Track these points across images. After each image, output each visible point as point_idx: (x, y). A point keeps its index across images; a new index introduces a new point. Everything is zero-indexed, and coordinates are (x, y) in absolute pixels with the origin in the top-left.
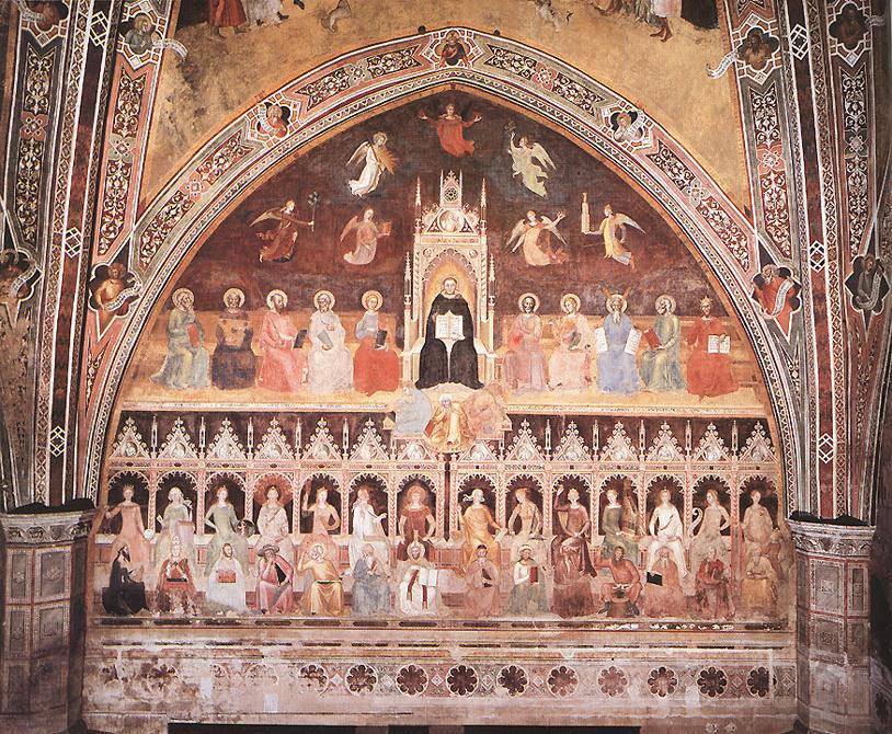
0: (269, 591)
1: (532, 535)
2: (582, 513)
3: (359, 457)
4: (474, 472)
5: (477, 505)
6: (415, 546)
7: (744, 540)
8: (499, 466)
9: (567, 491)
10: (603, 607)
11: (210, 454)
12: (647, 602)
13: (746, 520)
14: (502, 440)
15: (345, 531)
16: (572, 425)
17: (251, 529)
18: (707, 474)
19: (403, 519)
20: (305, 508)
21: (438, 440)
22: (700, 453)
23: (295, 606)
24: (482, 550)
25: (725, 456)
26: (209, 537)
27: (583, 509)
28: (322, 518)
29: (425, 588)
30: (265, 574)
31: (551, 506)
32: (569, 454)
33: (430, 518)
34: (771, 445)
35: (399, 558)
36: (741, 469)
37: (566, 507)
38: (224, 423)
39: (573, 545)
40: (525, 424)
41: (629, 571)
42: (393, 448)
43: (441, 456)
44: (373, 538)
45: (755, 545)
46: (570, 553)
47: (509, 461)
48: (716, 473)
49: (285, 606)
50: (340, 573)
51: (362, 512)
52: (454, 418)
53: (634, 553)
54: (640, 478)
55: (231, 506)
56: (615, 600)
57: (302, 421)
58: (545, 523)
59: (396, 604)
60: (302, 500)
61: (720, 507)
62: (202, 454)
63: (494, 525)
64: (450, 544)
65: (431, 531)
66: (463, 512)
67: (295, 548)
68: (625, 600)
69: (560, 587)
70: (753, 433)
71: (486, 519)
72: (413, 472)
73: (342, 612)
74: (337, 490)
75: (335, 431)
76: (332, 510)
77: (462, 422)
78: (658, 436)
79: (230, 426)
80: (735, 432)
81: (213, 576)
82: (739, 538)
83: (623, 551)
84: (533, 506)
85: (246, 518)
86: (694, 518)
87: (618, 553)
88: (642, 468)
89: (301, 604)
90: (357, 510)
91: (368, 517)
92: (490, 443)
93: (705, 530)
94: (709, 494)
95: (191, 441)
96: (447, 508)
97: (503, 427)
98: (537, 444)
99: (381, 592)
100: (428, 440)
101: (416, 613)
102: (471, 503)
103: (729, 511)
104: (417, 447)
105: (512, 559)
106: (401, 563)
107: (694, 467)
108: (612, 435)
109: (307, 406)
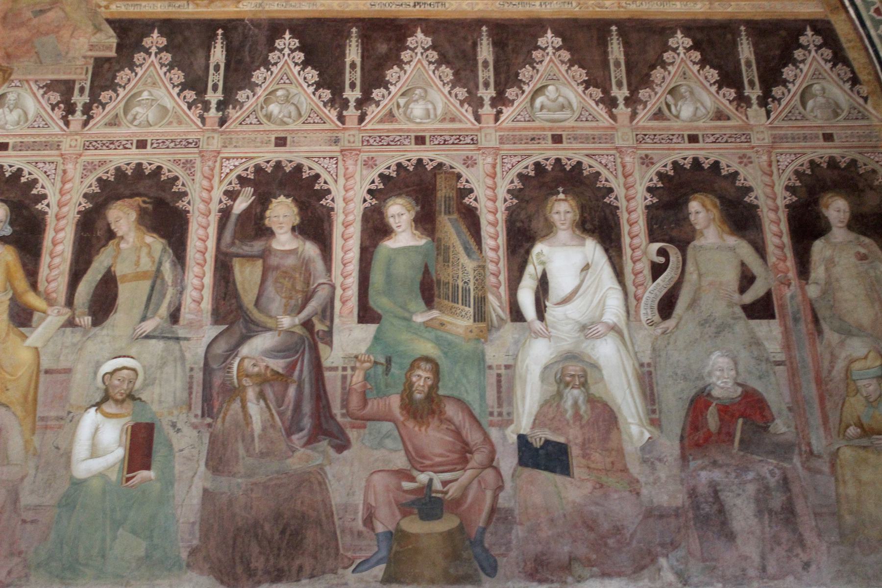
1: (149, 326)
2: (305, 265)
7: (820, 332)
9: (263, 200)
10: (370, 548)
12: (519, 532)
13: (818, 272)
16: (288, 41)
18: (686, 153)
22: (653, 105)
25: (730, 109)
27: (311, 249)
31: (211, 244)
32: (274, 108)
34: (855, 81)
36: (777, 140)
37: (258, 246)
39: (275, 352)
40: (155, 40)
41: (457, 433)
45: (857, 347)
46: (264, 380)
47: (98, 128)
48: (706, 153)
53: (473, 375)
54: (485, 162)
56: (414, 526)
58: (190, 294)
61: (732, 240)
63: (32, 299)
68: (447, 523)
69: (224, 484)
70: (798, 54)
78: (532, 63)
80: (746, 51)
82: (805, 327)
83: (436, 371)
84: (156, 243)
86: (657, 270)
87: (422, 379)
88: (490, 137)
92: (51, 86)
93: (693, 303)
94: (694, 206)
97: (92, 47)
98: (184, 87)
103: (760, 250)
105: (76, 395)
107: (641, 139)
108: (400, 63)
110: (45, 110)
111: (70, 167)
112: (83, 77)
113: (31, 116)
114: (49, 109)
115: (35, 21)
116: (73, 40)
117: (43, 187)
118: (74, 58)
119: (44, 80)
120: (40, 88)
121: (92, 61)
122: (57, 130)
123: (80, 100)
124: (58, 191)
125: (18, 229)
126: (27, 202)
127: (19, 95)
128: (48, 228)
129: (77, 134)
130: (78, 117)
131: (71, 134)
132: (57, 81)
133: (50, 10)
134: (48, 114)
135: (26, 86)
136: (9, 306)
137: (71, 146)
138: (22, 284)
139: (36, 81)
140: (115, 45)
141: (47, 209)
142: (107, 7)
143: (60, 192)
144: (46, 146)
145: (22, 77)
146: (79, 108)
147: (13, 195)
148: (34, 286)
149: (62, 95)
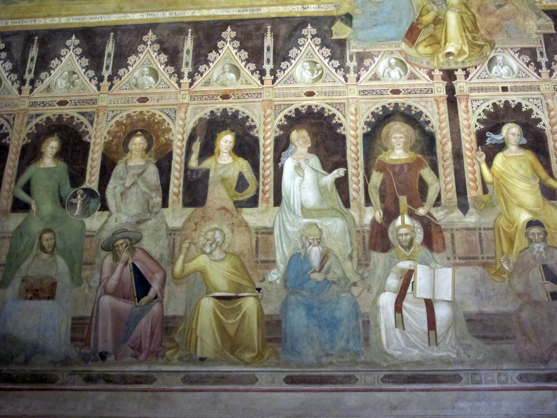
0: (116, 313)
3: (292, 79)
4: (500, 98)
5: (513, 149)
6: (403, 225)
8: (543, 86)
11: (40, 87)
14: (541, 47)
15: (267, 201)
17: (95, 203)
19: (377, 178)
20: (193, 163)
21: (429, 50)
23: (167, 344)
24: (535, 230)
26: (17, 219)
28: (224, 180)
29: (429, 304)
30: (113, 282)
33: (427, 173)
35: (374, 247)
38: (68, 42)
42: (352, 64)
43: (437, 73)
44: (317, 212)
49: (146, 344)
50: (255, 279)
51: (298, 168)
52: (452, 19)
55: (63, 165)
57: (195, 32)
59: (373, 337)
60: (189, 152)
62: (27, 87)
64: (471, 219)
65: (432, 195)
66: (489, 162)
67: (172, 232)
71: (534, 170)
72: (390, 100)
73: (260, 355)
74: (253, 133)
75: (250, 44)
76: (243, 165)
77: (468, 24)
79: (78, 46)
81: (16, 285)
85: (87, 185)
89: (177, 339)
90: (289, 164)
91: (309, 175)
92: (522, 52)
95: (13, 71)
96: (458, 156)
97: (539, 27)
99: (338, 314)
100: (411, 51)
101: (415, 354)
102: (502, 147)
104: (393, 61)
106: (378, 257)
109: (205, 12)
110: (524, 67)
111: (549, 101)
112: (539, 46)
113: (515, 69)
114: (525, 66)
115: (498, 12)
116: (527, 23)
117: (537, 114)
118: (530, 34)
119: (516, 48)
120: (515, 53)
121: (542, 36)
122: (534, 79)
123: (543, 60)
124: (547, 116)
125: (530, 139)
126: (530, 123)
127: (503, 57)
128: (548, 139)
129: (547, 81)
130: (544, 71)
131: (544, 81)
132: (525, 49)
133: (505, 4)
134: (526, 69)
135: (506, 51)
136: (540, 187)
137: (546, 88)
138: (543, 174)
139: (512, 49)
140: (553, 26)
141: (544, 128)
142: (540, 2)
143: (549, 117)
144: (531, 88)
145: (502, 46)
146: (543, 65)
147: (522, 119)
148: (551, 174)
149: (530, 57)
